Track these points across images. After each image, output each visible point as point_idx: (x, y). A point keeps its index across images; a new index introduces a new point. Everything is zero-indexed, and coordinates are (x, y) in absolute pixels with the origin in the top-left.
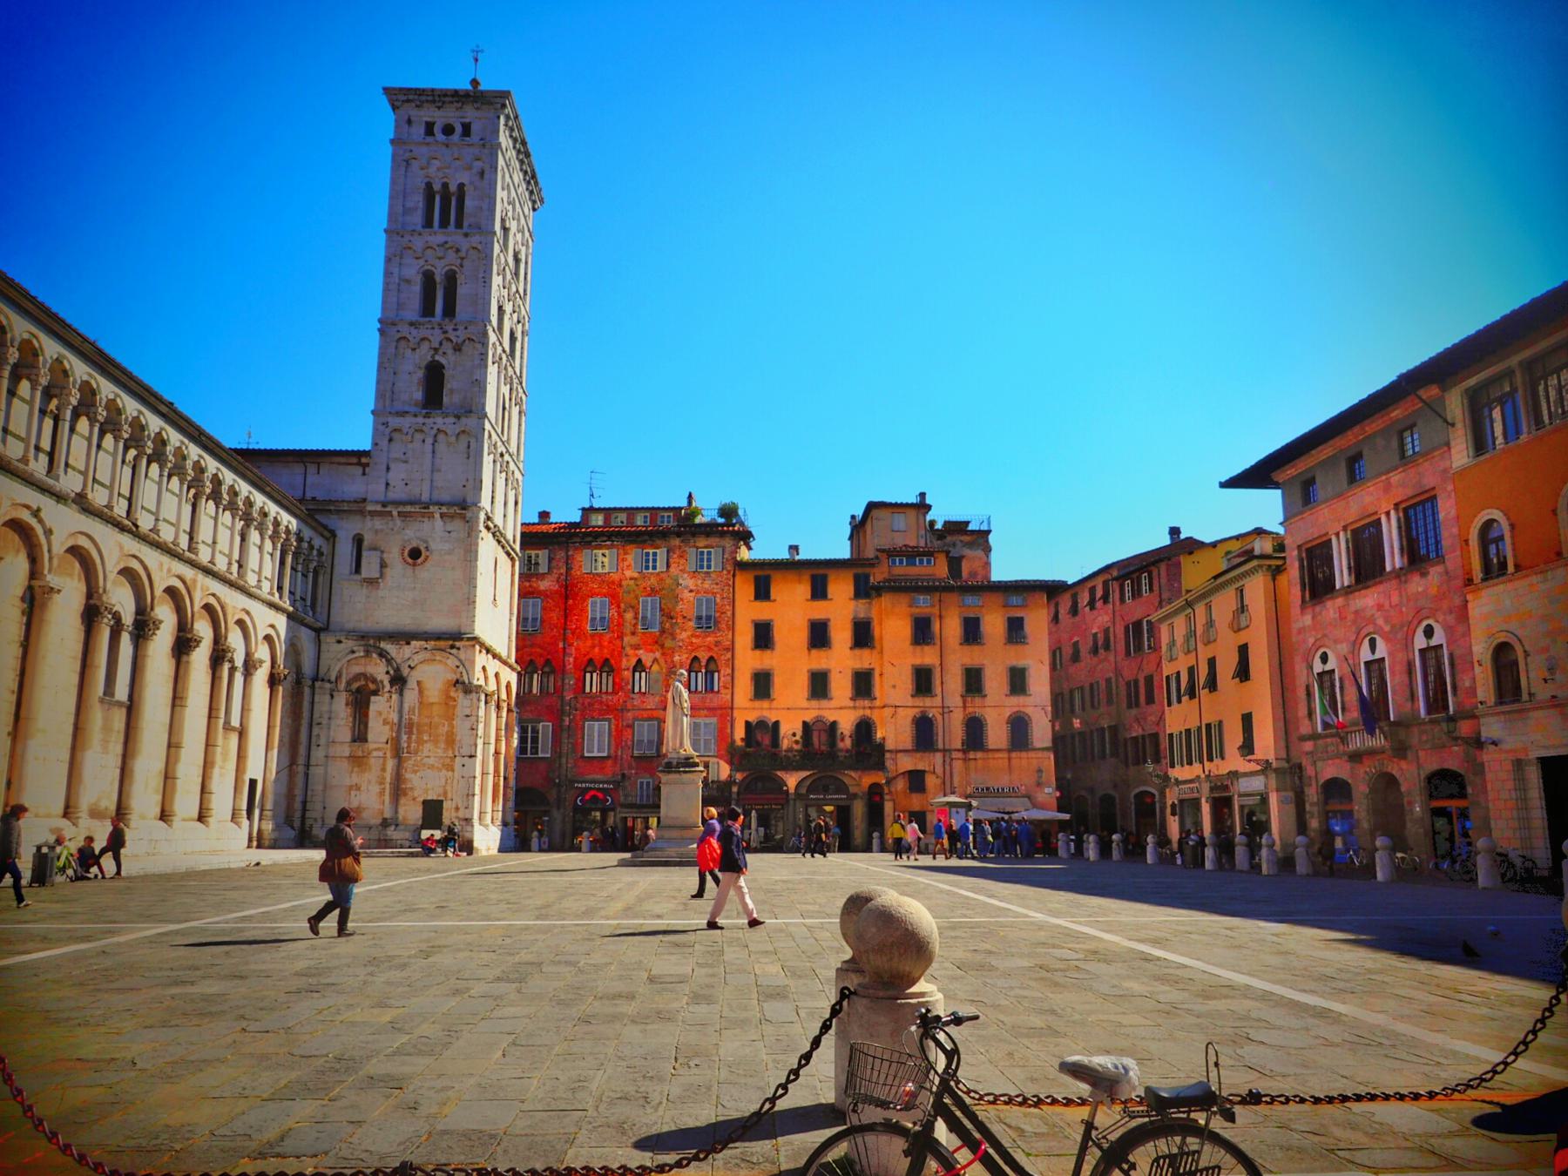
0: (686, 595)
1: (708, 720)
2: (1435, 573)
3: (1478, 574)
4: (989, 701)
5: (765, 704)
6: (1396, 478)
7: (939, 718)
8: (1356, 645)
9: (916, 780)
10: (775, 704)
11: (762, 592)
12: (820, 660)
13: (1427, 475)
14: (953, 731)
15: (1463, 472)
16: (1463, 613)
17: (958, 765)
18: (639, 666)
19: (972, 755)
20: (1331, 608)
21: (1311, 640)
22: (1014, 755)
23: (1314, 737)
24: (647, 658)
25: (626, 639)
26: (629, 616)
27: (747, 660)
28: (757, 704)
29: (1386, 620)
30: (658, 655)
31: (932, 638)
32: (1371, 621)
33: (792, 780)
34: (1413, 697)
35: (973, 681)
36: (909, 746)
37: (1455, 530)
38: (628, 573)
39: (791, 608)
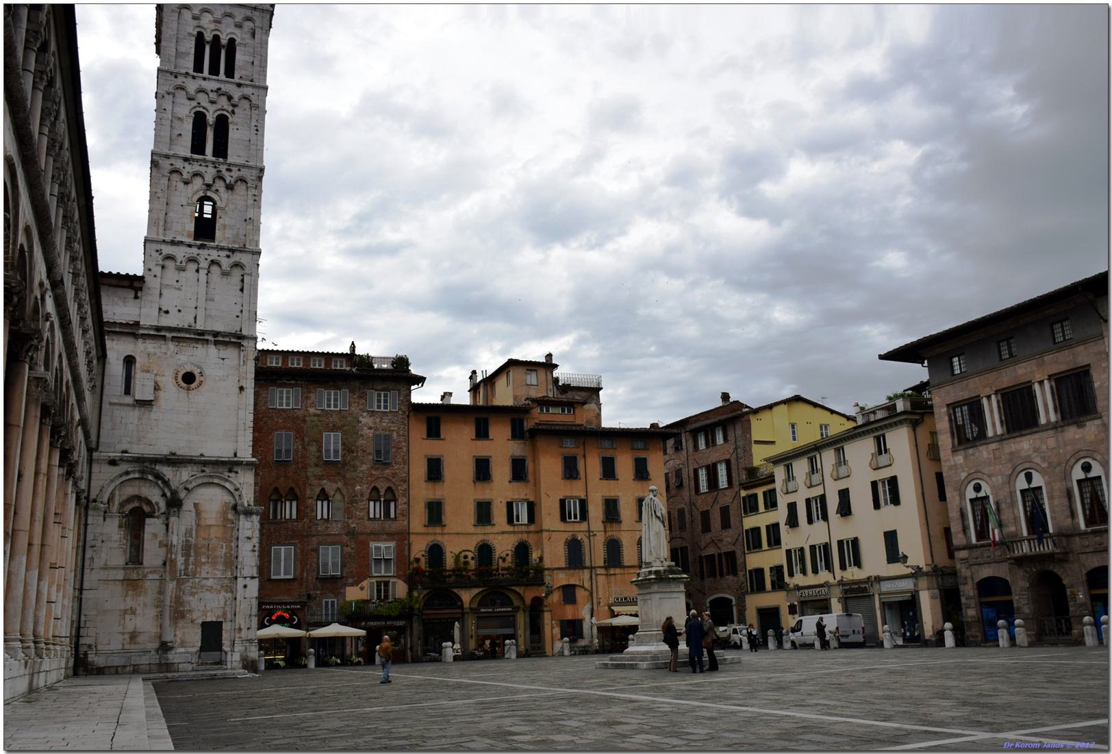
0: (366, 431)
1: (388, 545)
4: (624, 526)
5: (438, 530)
7: (586, 541)
9: (569, 593)
10: (446, 530)
11: (434, 432)
12: (484, 492)
14: (597, 553)
17: (601, 580)
18: (323, 496)
19: (612, 571)
24: (330, 487)
25: (311, 469)
26: (313, 449)
27: (421, 492)
28: (431, 530)
30: (340, 485)
31: (578, 474)
33: (466, 596)
36: (562, 563)
38: (312, 410)
39: (459, 448)
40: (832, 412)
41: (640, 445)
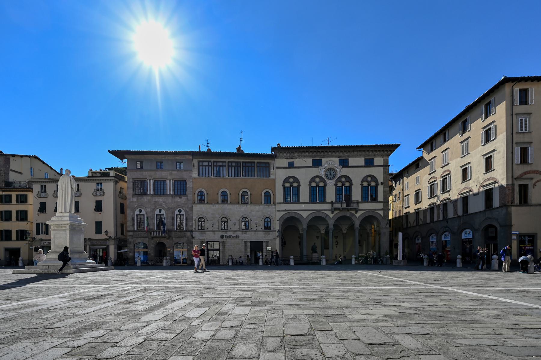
2: (184, 198)
3: (196, 202)
8: (154, 210)
13: (185, 175)
15: (195, 178)
16: (191, 209)
20: (145, 199)
21: (136, 206)
23: (134, 231)
29: (166, 206)
34: (173, 225)
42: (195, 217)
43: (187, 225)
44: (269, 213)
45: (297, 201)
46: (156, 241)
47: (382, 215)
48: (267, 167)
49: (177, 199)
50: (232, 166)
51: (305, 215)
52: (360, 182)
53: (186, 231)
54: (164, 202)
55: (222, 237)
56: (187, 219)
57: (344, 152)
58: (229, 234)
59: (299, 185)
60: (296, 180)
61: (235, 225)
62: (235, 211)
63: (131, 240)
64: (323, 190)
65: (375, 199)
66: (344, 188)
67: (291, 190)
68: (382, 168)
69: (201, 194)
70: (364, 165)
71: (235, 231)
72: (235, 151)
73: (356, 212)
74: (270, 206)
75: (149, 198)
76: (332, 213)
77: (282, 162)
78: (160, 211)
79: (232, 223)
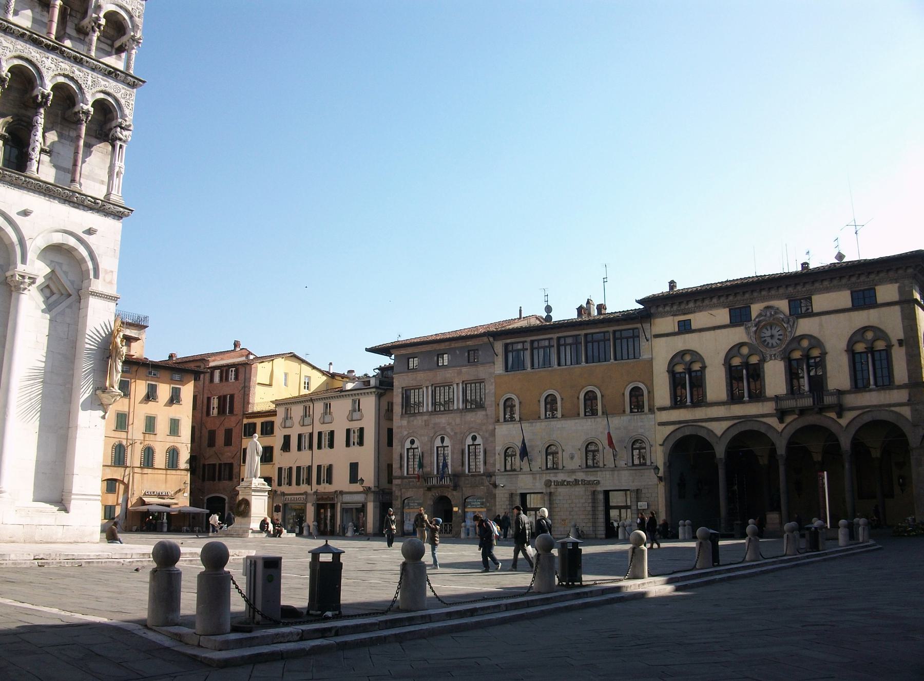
3: (502, 419)
6: (464, 370)
8: (432, 441)
14: (135, 457)
15: (500, 376)
16: (493, 433)
19: (146, 471)
20: (419, 421)
21: (406, 433)
22: (169, 472)
29: (452, 430)
32: (444, 429)
34: (463, 464)
35: (150, 424)
37: (493, 399)
40: (314, 368)
41: (177, 377)
42: (499, 448)
43: (485, 463)
44: (641, 431)
45: (699, 401)
46: (436, 493)
47: (909, 417)
48: (635, 337)
49: (470, 417)
50: (565, 345)
51: (718, 428)
52: (843, 345)
53: (484, 475)
54: (449, 424)
55: (548, 483)
56: (485, 452)
57: (802, 284)
58: (561, 477)
59: (704, 368)
60: (696, 356)
61: (572, 458)
62: (572, 433)
63: (397, 492)
64: (756, 373)
65: (886, 382)
66: (805, 362)
67: (687, 380)
68: (897, 308)
69: (508, 405)
70: (849, 304)
71: (573, 472)
72: (574, 315)
73: (840, 416)
74: (643, 416)
75: (425, 418)
76: (781, 420)
77: (666, 323)
78: (443, 440)
79: (566, 455)
